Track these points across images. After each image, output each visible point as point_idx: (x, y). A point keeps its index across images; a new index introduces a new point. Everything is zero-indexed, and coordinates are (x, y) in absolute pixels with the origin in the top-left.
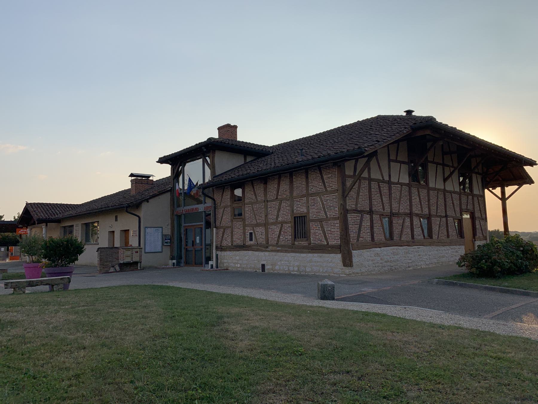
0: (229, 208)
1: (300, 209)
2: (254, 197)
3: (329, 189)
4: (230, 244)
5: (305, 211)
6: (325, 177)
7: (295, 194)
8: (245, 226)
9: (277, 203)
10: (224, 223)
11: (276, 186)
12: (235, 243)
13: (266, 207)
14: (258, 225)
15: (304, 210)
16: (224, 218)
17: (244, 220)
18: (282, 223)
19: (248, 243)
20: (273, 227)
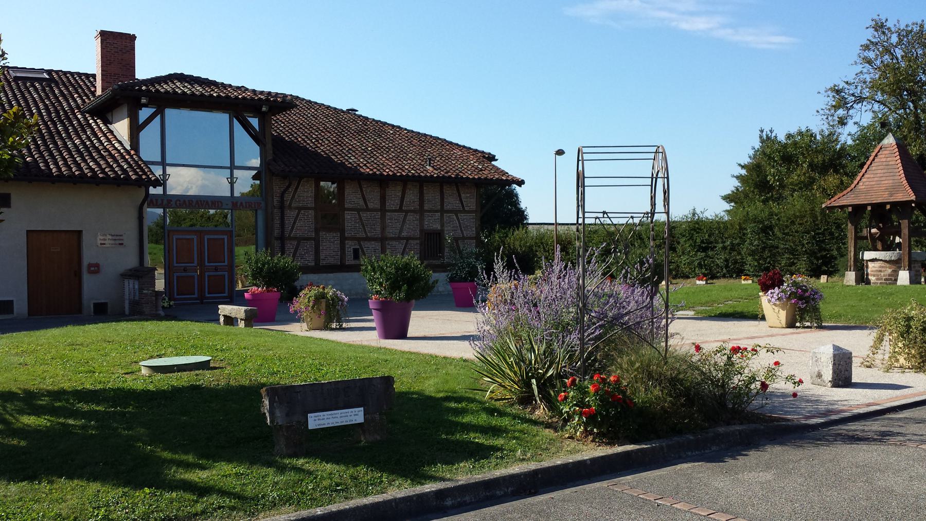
0: (312, 212)
1: (432, 223)
2: (362, 202)
3: (466, 209)
4: (313, 264)
5: (439, 228)
6: (463, 195)
7: (426, 208)
8: (343, 240)
9: (402, 215)
10: (296, 233)
11: (400, 194)
12: (323, 263)
13: (383, 217)
14: (368, 239)
15: (437, 226)
16: (298, 224)
17: (343, 231)
18: (408, 239)
19: (349, 260)
20: (394, 243)
